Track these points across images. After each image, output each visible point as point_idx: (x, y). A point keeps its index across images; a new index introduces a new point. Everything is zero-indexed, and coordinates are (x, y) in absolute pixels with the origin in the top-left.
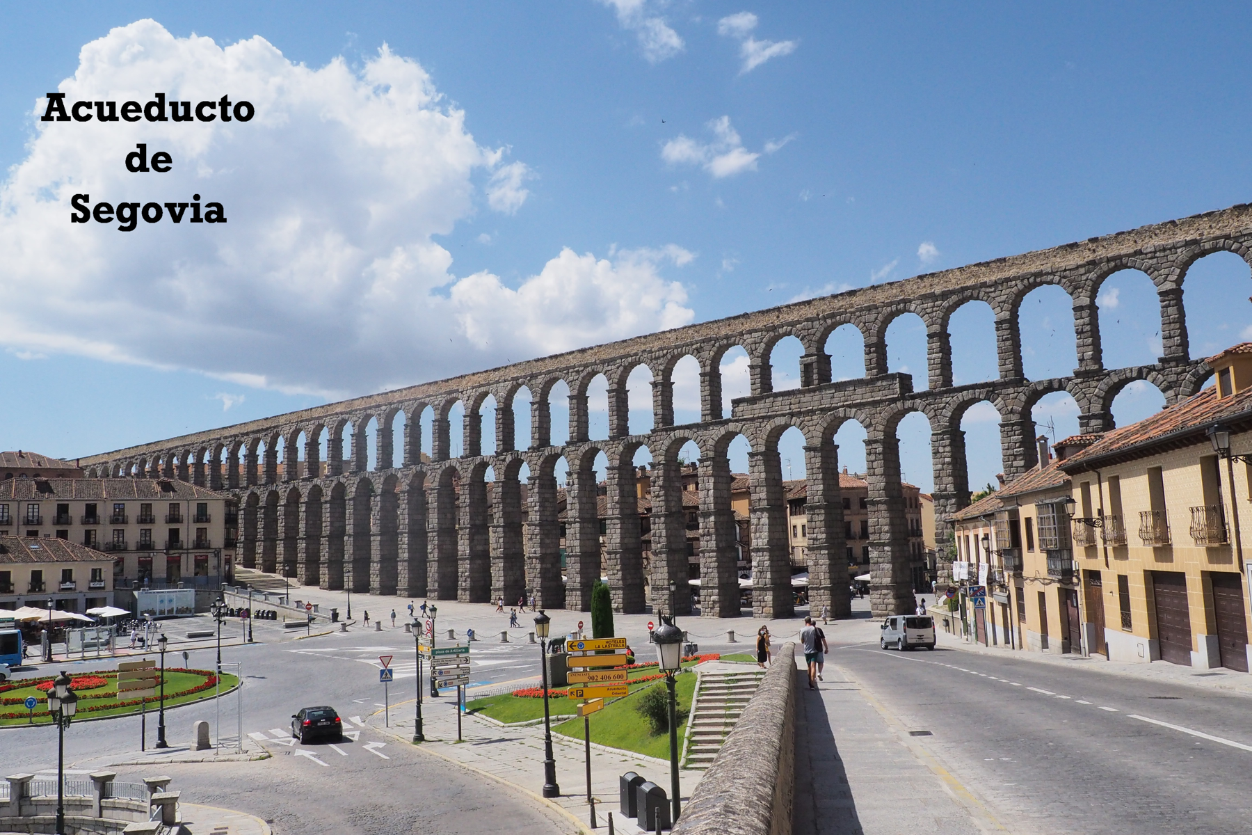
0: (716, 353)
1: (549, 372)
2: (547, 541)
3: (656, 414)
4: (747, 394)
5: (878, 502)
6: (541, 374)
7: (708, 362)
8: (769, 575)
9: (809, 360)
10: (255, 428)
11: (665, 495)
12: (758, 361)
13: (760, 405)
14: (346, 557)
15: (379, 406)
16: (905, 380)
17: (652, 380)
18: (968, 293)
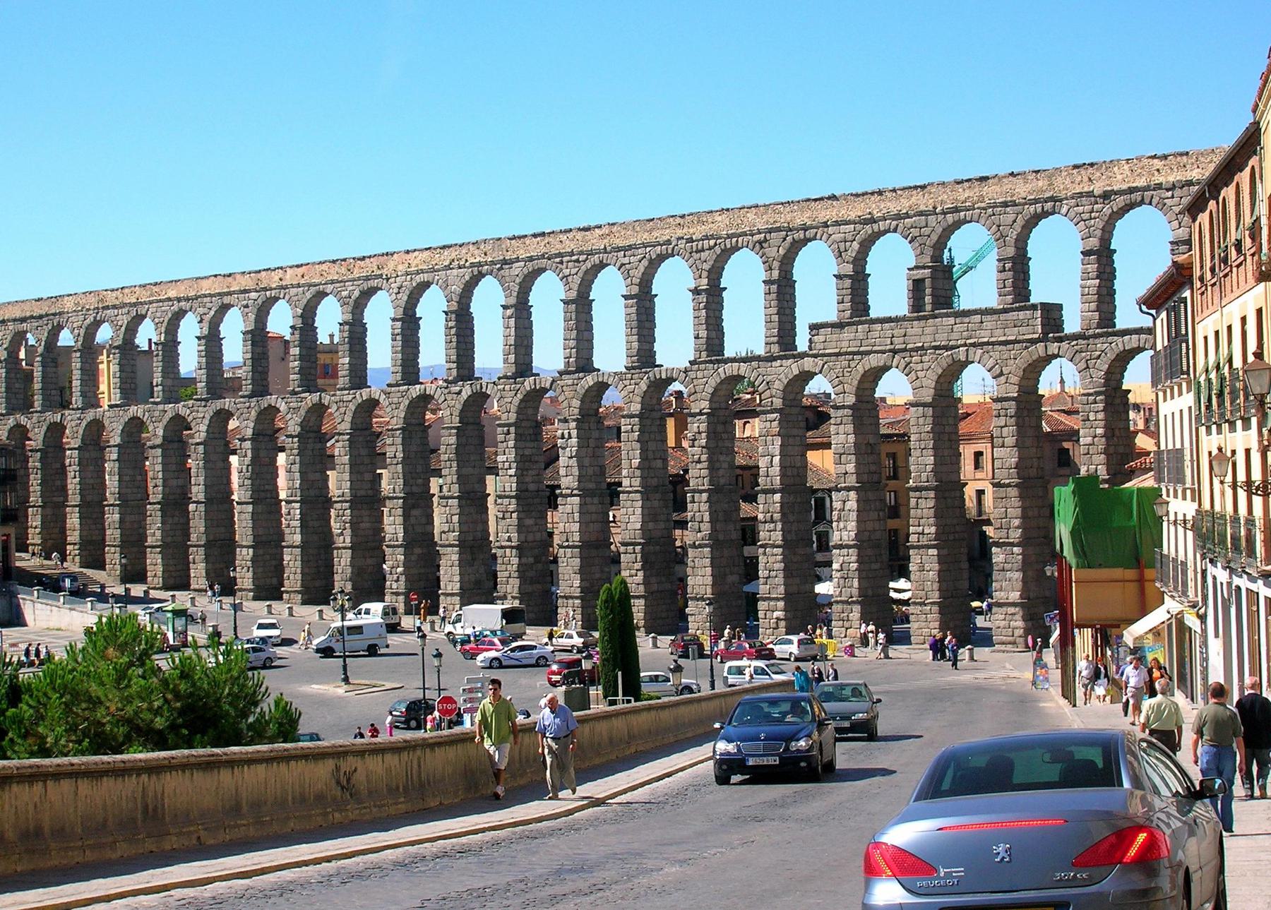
0: (789, 251)
1: (531, 259)
2: (529, 522)
3: (697, 337)
4: (832, 317)
5: (1009, 485)
6: (517, 260)
7: (776, 264)
8: (856, 584)
9: (919, 274)
10: (18, 314)
11: (710, 460)
12: (848, 269)
13: (848, 334)
14: (194, 537)
15: (245, 291)
16: (1052, 315)
17: (692, 286)
18: (1137, 196)
